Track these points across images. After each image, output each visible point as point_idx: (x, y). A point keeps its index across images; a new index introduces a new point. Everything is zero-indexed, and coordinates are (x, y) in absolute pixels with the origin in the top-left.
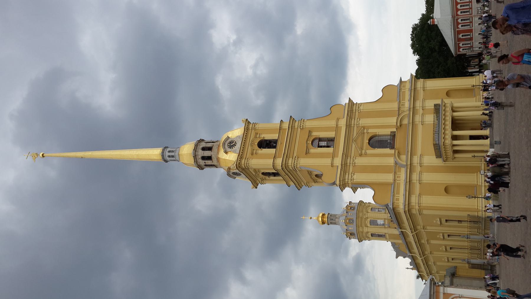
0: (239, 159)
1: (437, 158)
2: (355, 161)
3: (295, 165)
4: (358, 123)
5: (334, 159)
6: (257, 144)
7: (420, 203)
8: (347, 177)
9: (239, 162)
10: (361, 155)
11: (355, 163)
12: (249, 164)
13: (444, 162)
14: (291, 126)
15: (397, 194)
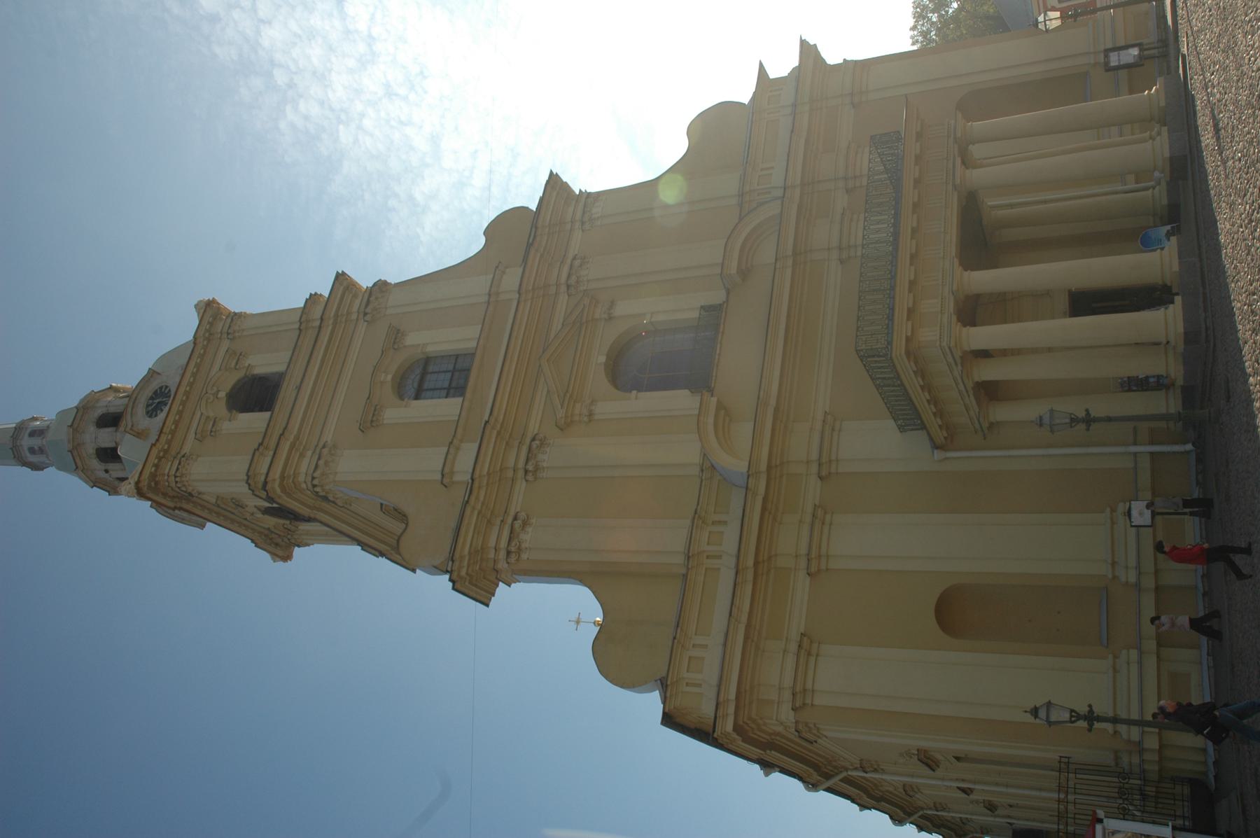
0: (153, 460)
1: (902, 429)
2: (540, 457)
3: (316, 482)
4: (574, 278)
5: (458, 449)
6: (222, 394)
7: (805, 690)
8: (492, 543)
9: (153, 469)
10: (565, 426)
11: (537, 469)
12: (184, 479)
13: (938, 455)
14: (332, 314)
15: (696, 634)
